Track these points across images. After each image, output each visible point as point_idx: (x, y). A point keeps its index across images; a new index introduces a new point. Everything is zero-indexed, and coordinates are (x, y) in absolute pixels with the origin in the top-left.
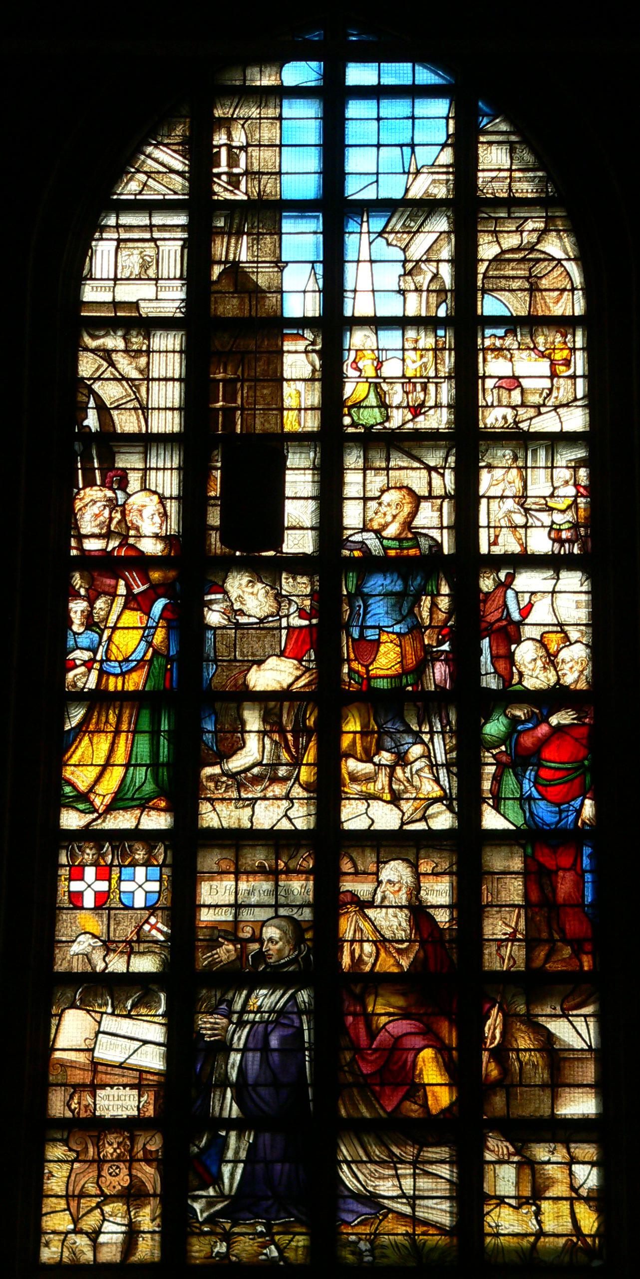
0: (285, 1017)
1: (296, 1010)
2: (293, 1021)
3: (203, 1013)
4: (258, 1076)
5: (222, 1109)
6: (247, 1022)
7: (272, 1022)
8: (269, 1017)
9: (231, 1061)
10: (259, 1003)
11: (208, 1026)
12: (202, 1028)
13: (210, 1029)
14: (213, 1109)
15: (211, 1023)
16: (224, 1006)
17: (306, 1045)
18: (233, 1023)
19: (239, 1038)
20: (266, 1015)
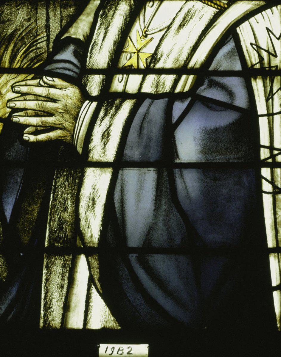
0: (213, 84)
1: (238, 67)
2: (231, 94)
3: (19, 71)
4: (150, 230)
5: (66, 308)
6: (124, 96)
7: (182, 96)
8: (176, 83)
9: (86, 192)
10: (150, 50)
11: (32, 104)
12: (15, 110)
13: (36, 114)
14: (48, 307)
15: (37, 97)
16: (68, 54)
17: (264, 154)
18: (92, 99)
19: (106, 135)
20: (168, 80)
